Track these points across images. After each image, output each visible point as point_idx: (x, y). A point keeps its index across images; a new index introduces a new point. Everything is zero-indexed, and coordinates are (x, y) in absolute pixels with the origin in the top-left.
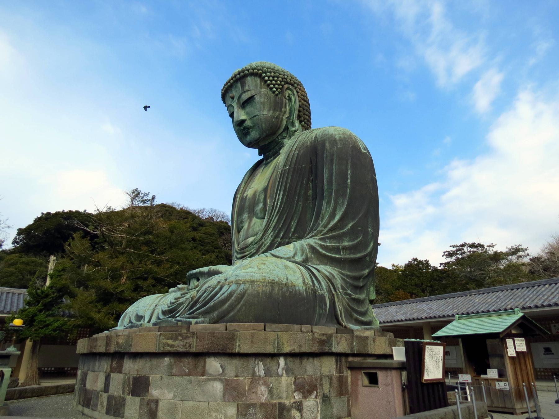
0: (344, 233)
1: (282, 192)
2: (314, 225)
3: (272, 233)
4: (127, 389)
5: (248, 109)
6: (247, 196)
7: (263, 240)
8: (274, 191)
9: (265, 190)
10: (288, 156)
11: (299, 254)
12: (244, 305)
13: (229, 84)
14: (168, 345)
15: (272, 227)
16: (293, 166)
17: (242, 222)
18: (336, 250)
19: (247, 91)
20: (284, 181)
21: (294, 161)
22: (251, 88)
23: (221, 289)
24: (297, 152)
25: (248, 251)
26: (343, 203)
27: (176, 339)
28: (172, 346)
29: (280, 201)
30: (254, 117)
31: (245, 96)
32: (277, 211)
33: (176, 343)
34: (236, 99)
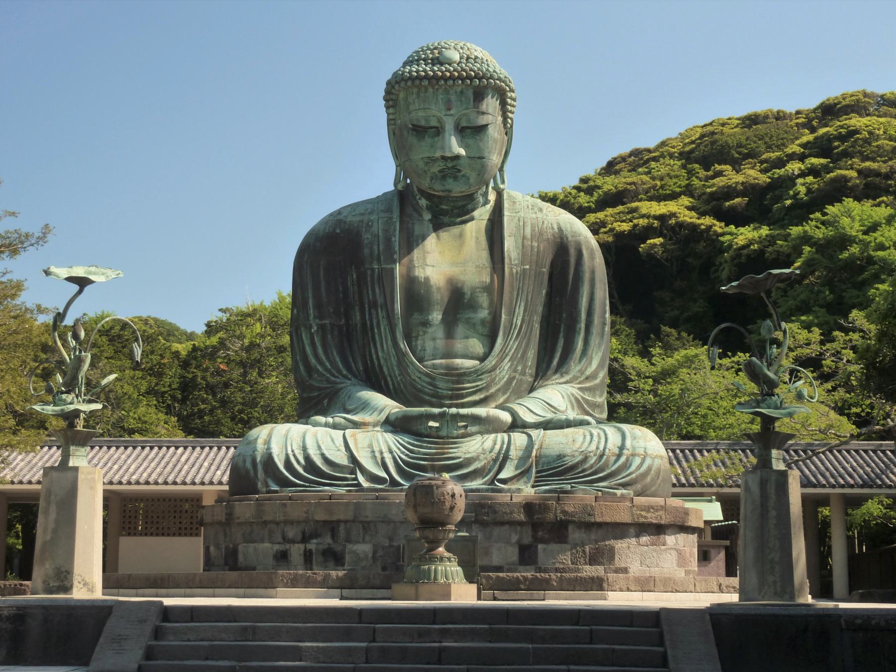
0: (597, 385)
1: (523, 304)
4: (582, 560)
6: (427, 279)
7: (498, 371)
10: (523, 246)
11: (569, 407)
14: (642, 516)
18: (594, 406)
21: (534, 258)
22: (490, 111)
24: (535, 244)
25: (469, 382)
27: (648, 511)
28: (645, 517)
29: (520, 318)
33: (649, 515)
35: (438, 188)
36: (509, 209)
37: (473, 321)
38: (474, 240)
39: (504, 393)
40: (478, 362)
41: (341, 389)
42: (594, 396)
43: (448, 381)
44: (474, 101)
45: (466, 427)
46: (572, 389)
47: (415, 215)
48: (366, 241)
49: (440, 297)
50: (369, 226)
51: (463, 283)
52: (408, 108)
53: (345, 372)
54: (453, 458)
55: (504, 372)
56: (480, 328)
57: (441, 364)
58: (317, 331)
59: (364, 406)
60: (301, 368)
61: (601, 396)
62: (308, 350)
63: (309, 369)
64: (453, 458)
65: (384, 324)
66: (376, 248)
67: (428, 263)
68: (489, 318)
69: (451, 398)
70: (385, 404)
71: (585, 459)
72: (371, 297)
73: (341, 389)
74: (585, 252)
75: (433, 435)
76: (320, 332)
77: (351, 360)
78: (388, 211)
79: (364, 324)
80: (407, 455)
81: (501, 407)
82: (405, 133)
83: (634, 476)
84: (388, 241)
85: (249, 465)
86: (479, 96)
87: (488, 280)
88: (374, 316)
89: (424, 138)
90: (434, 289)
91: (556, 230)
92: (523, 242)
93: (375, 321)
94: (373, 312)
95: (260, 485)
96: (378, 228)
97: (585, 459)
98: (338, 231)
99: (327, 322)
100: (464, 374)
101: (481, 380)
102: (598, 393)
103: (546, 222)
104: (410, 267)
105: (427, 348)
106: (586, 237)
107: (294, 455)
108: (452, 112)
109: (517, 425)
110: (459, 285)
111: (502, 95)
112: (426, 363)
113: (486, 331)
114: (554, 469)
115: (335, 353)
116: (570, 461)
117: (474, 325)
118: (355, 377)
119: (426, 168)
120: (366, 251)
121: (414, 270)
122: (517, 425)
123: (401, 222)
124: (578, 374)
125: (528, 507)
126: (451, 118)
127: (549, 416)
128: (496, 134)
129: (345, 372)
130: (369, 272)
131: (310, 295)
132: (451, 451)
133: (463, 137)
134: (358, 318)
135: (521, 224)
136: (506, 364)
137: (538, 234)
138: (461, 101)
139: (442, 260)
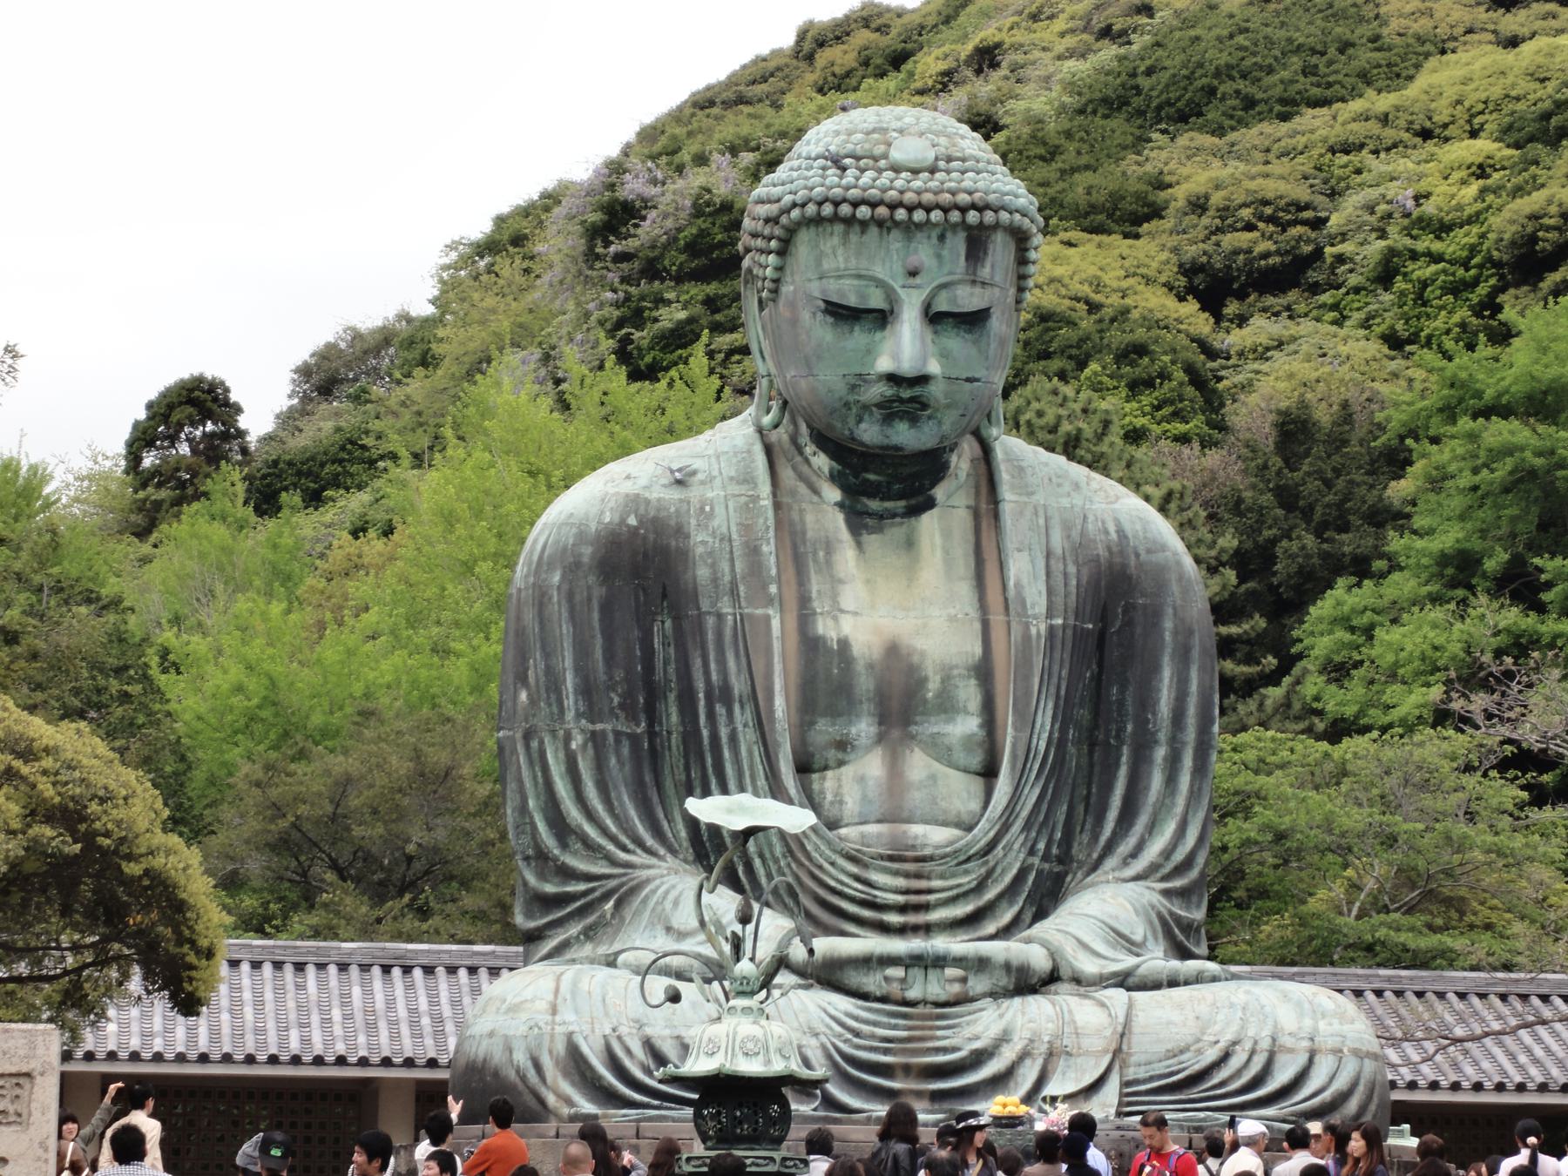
1: (1051, 705)
2: (1114, 833)
3: (1022, 837)
5: (956, 342)
6: (844, 644)
8: (1028, 693)
9: (983, 672)
10: (1048, 574)
11: (1150, 937)
12: (1379, 1106)
13: (919, 216)
15: (1025, 813)
16: (1071, 622)
17: (843, 745)
19: (983, 283)
20: (1056, 668)
22: (998, 279)
23: (1311, 1061)
24: (1072, 569)
25: (942, 877)
26: (1200, 789)
29: (1045, 735)
30: (968, 380)
31: (968, 299)
32: (1036, 766)
34: (926, 284)
36: (1013, 487)
37: (946, 741)
38: (939, 553)
39: (1011, 903)
40: (956, 832)
41: (648, 881)
42: (1188, 909)
43: (896, 873)
44: (967, 258)
45: (964, 980)
46: (1149, 894)
47: (803, 489)
48: (700, 550)
50: (705, 515)
51: (923, 654)
52: (819, 263)
53: (650, 841)
54: (945, 1050)
56: (960, 757)
57: (879, 835)
58: (584, 746)
60: (542, 827)
61: (1198, 906)
62: (562, 788)
63: (561, 827)
64: (945, 1050)
65: (747, 737)
66: (725, 567)
67: (844, 606)
68: (982, 733)
69: (903, 909)
71: (1225, 1057)
72: (714, 677)
73: (648, 881)
74: (1175, 588)
76: (590, 751)
77: (661, 816)
78: (745, 481)
79: (691, 735)
80: (846, 1041)
82: (806, 316)
83: (1326, 1096)
84: (753, 551)
85: (520, 1057)
87: (978, 650)
88: (722, 720)
89: (852, 331)
90: (860, 667)
91: (1114, 536)
92: (1048, 566)
93: (724, 732)
94: (720, 710)
95: (551, 1099)
97: (1225, 1057)
98: (632, 521)
99: (608, 727)
100: (931, 858)
101: (967, 872)
102: (1194, 899)
103: (1091, 518)
104: (805, 617)
105: (847, 799)
106: (1175, 554)
107: (619, 1038)
108: (918, 280)
110: (916, 659)
112: (843, 831)
113: (976, 760)
115: (626, 798)
117: (950, 749)
118: (673, 852)
119: (851, 398)
120: (703, 573)
121: (814, 622)
123: (777, 506)
124: (1161, 860)
126: (914, 292)
128: (1004, 327)
129: (650, 841)
130: (710, 621)
131: (568, 662)
132: (939, 1033)
133: (936, 332)
134: (674, 718)
135: (1042, 521)
137: (1080, 547)
138: (939, 256)
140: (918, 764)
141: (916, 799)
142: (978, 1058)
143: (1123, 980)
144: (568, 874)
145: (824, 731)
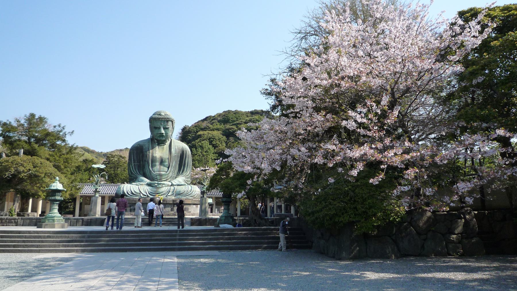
18: (187, 181)
35: (159, 139)
46: (184, 178)
49: (158, 160)
55: (171, 174)
59: (142, 181)
63: (132, 173)
70: (147, 181)
75: (156, 187)
81: (169, 182)
86: (167, 121)
96: (147, 146)
104: (153, 154)
109: (172, 185)
111: (172, 122)
114: (179, 194)
116: (181, 192)
122: (172, 185)
125: (173, 201)
127: (179, 183)
136: (171, 173)
137: (179, 148)
139: (159, 152)
140: (162, 167)
141: (162, 170)
142: (162, 192)
143: (178, 185)
144: (132, 177)
145: (154, 164)
